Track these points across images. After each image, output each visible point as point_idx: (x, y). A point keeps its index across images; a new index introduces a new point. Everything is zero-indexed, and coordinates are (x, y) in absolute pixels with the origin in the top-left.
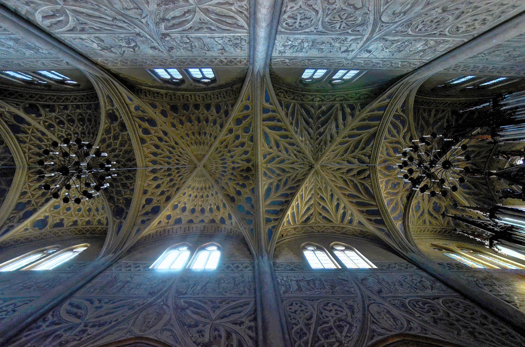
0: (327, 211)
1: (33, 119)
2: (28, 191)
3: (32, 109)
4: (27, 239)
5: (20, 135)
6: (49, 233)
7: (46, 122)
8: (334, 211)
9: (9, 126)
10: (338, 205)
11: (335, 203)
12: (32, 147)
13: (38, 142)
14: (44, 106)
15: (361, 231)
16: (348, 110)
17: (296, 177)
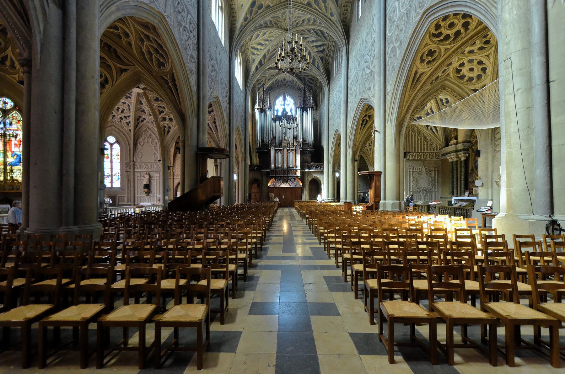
0: (257, 38)
8: (258, 42)
10: (262, 45)
11: (263, 42)
15: (249, 61)
16: (321, 49)
17: (279, 21)
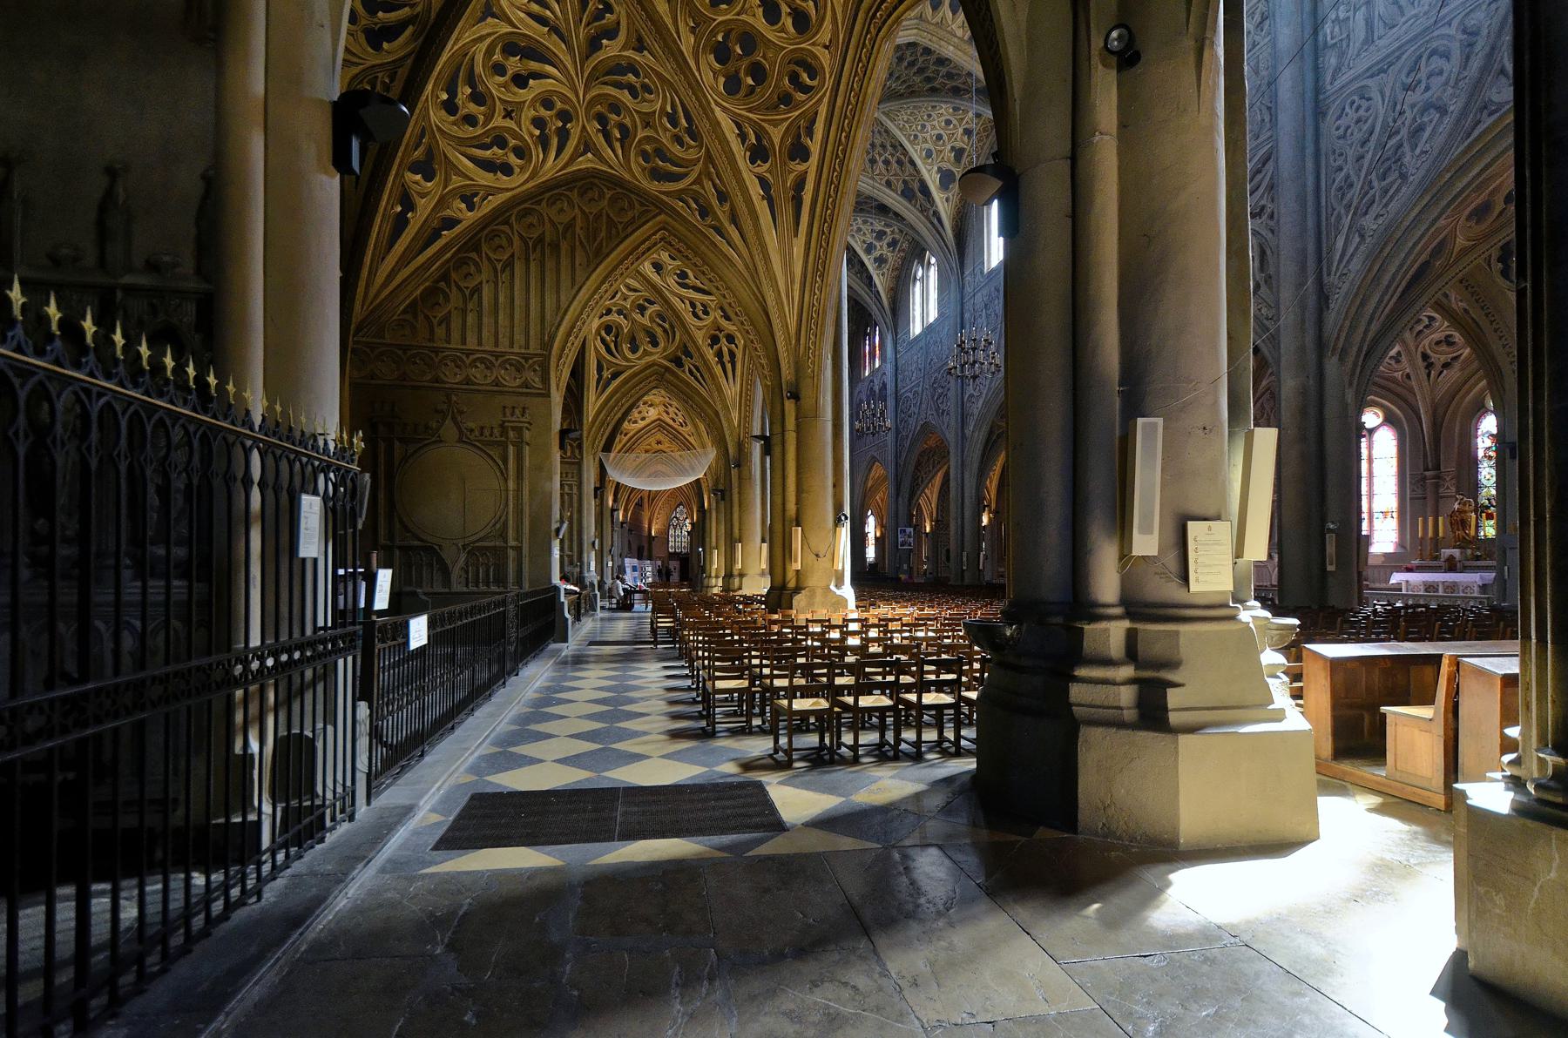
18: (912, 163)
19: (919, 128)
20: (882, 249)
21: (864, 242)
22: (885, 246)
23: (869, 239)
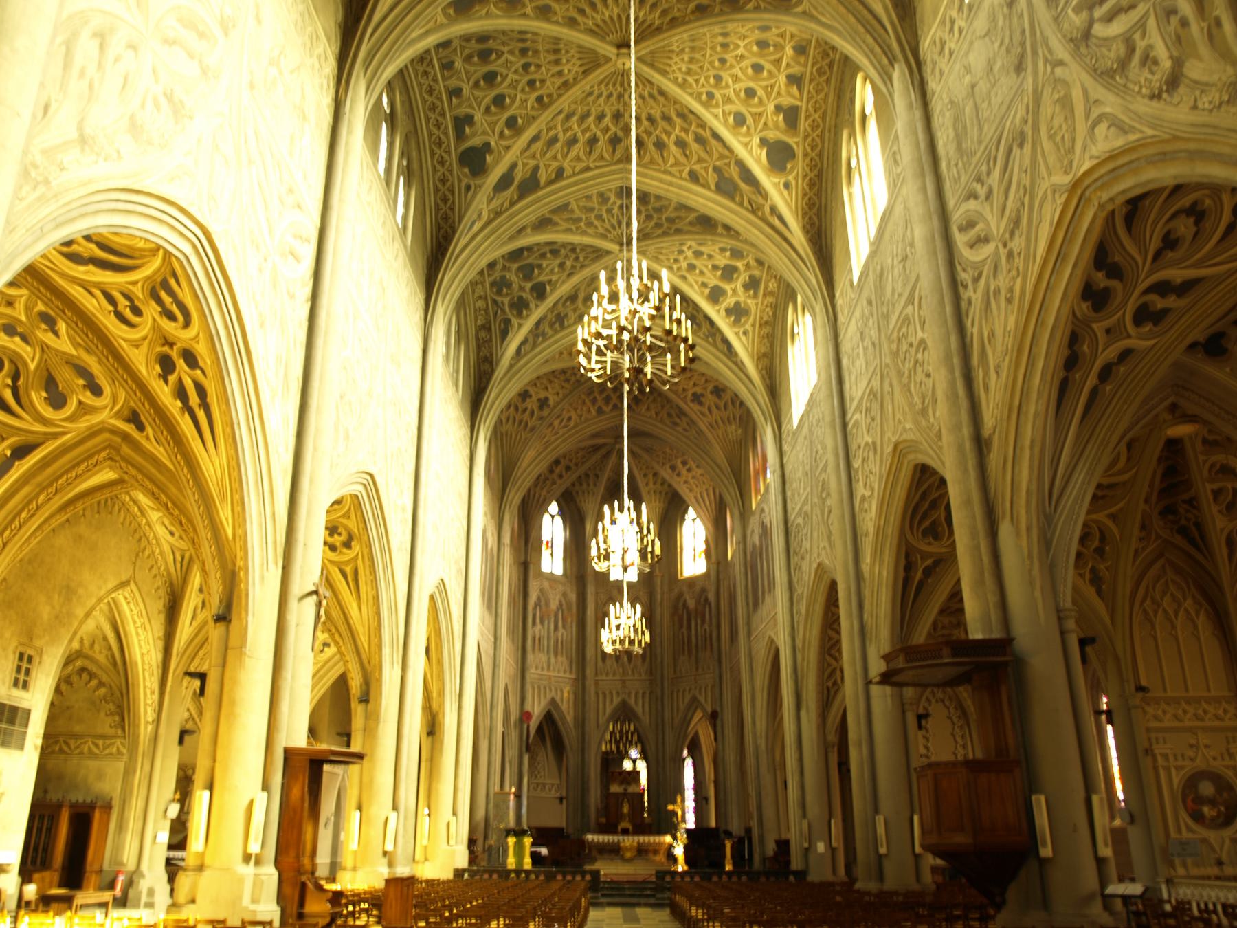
1: (498, 161)
2: (687, 169)
3: (475, 160)
4: (812, 185)
5: (543, 181)
6: (809, 139)
7: (501, 134)
9: (521, 197)
12: (572, 155)
13: (559, 145)
14: (460, 135)
18: (716, 136)
19: (712, 81)
20: (735, 293)
21: (704, 285)
22: (740, 290)
23: (713, 280)
